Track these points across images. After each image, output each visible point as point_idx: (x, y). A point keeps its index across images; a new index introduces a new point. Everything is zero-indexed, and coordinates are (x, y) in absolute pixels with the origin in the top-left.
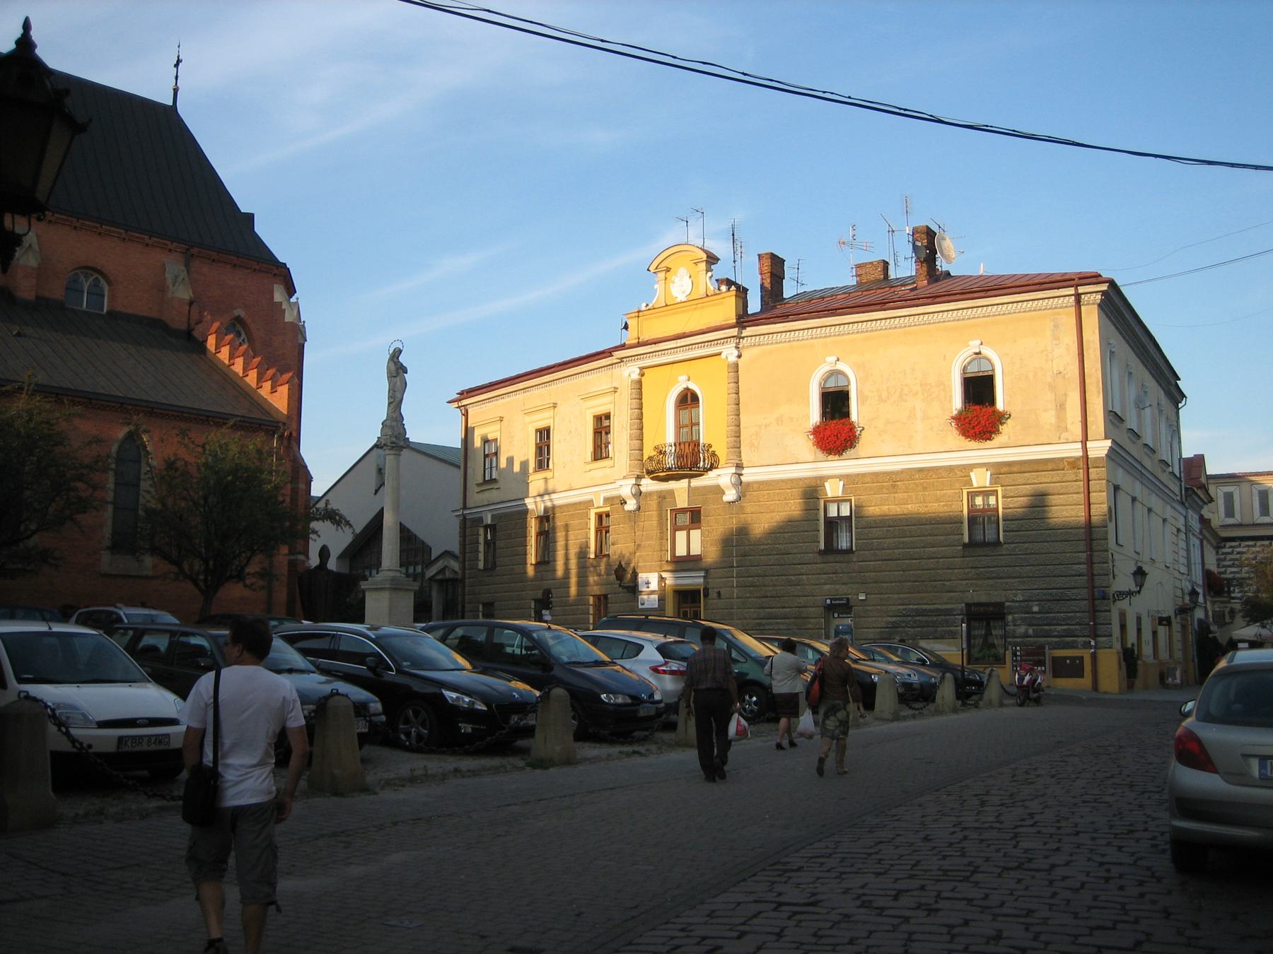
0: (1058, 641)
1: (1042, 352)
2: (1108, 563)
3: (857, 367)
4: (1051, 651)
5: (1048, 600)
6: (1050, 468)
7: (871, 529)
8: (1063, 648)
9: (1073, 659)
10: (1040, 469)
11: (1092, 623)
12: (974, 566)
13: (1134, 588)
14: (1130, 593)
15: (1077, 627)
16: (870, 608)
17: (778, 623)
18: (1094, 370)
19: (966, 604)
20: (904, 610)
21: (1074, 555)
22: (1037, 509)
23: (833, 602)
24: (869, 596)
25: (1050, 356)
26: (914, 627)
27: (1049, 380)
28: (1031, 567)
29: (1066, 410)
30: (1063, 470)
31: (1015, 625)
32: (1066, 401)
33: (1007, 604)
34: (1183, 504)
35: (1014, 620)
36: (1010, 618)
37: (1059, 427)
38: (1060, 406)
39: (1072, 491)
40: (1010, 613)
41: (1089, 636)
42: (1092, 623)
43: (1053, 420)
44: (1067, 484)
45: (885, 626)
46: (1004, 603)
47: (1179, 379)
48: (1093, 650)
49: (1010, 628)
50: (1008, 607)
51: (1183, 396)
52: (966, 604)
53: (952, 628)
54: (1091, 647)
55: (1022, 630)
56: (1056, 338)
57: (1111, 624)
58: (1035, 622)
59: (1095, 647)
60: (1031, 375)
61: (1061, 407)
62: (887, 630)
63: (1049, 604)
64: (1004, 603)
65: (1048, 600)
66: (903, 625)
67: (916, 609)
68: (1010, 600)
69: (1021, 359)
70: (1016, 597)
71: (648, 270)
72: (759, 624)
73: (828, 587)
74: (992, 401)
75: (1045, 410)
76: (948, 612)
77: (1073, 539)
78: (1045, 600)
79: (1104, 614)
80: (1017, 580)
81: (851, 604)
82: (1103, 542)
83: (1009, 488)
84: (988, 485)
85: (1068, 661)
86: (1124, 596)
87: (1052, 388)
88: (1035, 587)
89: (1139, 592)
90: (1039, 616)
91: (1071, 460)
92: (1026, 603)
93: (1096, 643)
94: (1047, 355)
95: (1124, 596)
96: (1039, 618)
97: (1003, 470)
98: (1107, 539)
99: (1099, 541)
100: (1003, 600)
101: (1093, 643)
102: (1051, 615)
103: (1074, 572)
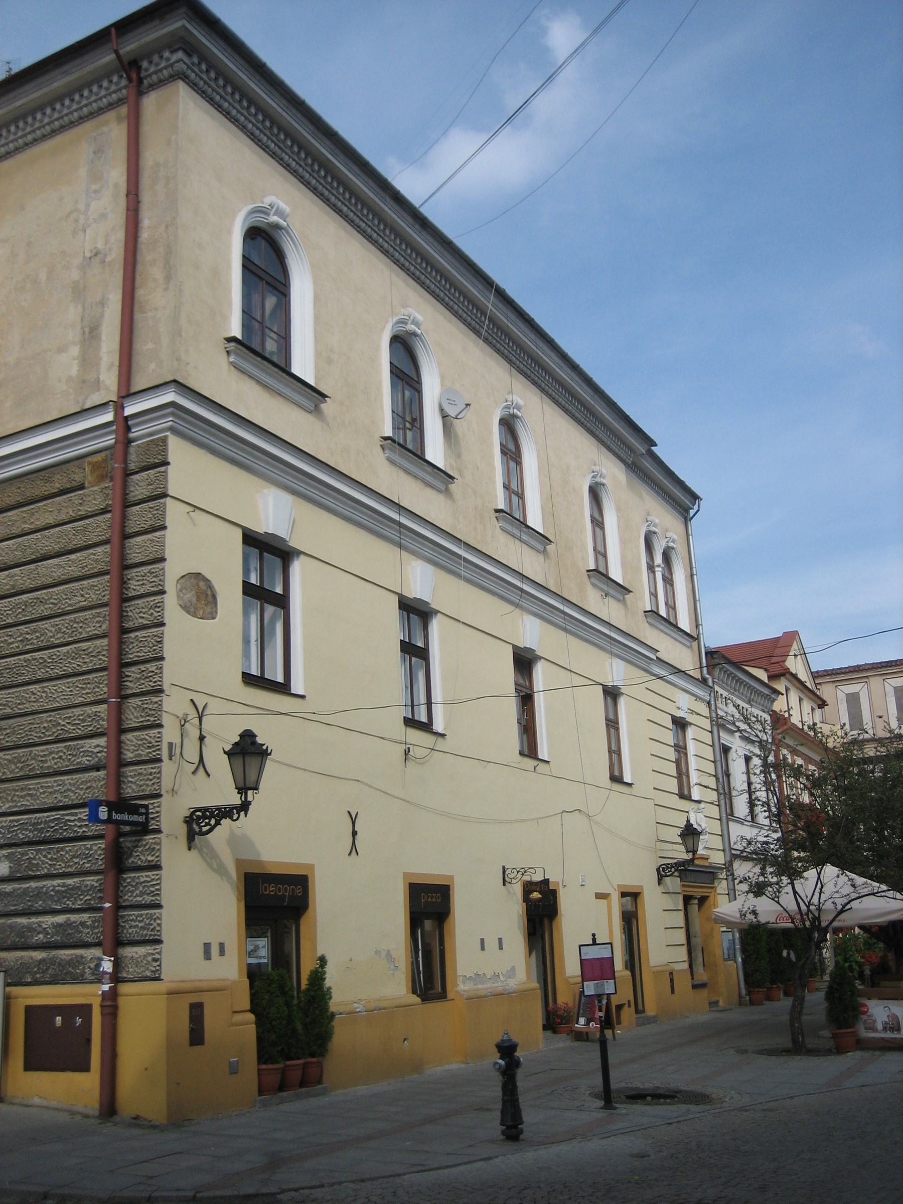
0: (42, 961)
1: (68, 216)
2: (160, 726)
5: (30, 843)
6: (57, 486)
8: (53, 982)
9: (68, 1011)
10: (37, 493)
11: (107, 905)
14: (226, 813)
15: (85, 917)
18: (162, 228)
22: (24, 597)
27: (75, 275)
29: (100, 339)
30: (82, 487)
32: (102, 316)
34: (704, 681)
37: (84, 382)
39: (96, 540)
41: (98, 944)
42: (107, 905)
43: (74, 371)
44: (87, 521)
47: (656, 445)
48: (106, 987)
51: (695, 497)
54: (99, 979)
56: (96, 176)
59: (116, 978)
60: (43, 276)
61: (91, 333)
63: (31, 852)
65: (30, 843)
69: (29, 244)
75: (62, 349)
77: (90, 666)
79: (143, 876)
82: (152, 667)
85: (59, 1020)
86: (213, 822)
87: (78, 291)
89: (244, 807)
91: (98, 458)
93: (117, 964)
94: (76, 221)
95: (213, 822)
98: (162, 658)
99: (142, 668)
101: (107, 966)
102: (33, 884)
103: (85, 761)
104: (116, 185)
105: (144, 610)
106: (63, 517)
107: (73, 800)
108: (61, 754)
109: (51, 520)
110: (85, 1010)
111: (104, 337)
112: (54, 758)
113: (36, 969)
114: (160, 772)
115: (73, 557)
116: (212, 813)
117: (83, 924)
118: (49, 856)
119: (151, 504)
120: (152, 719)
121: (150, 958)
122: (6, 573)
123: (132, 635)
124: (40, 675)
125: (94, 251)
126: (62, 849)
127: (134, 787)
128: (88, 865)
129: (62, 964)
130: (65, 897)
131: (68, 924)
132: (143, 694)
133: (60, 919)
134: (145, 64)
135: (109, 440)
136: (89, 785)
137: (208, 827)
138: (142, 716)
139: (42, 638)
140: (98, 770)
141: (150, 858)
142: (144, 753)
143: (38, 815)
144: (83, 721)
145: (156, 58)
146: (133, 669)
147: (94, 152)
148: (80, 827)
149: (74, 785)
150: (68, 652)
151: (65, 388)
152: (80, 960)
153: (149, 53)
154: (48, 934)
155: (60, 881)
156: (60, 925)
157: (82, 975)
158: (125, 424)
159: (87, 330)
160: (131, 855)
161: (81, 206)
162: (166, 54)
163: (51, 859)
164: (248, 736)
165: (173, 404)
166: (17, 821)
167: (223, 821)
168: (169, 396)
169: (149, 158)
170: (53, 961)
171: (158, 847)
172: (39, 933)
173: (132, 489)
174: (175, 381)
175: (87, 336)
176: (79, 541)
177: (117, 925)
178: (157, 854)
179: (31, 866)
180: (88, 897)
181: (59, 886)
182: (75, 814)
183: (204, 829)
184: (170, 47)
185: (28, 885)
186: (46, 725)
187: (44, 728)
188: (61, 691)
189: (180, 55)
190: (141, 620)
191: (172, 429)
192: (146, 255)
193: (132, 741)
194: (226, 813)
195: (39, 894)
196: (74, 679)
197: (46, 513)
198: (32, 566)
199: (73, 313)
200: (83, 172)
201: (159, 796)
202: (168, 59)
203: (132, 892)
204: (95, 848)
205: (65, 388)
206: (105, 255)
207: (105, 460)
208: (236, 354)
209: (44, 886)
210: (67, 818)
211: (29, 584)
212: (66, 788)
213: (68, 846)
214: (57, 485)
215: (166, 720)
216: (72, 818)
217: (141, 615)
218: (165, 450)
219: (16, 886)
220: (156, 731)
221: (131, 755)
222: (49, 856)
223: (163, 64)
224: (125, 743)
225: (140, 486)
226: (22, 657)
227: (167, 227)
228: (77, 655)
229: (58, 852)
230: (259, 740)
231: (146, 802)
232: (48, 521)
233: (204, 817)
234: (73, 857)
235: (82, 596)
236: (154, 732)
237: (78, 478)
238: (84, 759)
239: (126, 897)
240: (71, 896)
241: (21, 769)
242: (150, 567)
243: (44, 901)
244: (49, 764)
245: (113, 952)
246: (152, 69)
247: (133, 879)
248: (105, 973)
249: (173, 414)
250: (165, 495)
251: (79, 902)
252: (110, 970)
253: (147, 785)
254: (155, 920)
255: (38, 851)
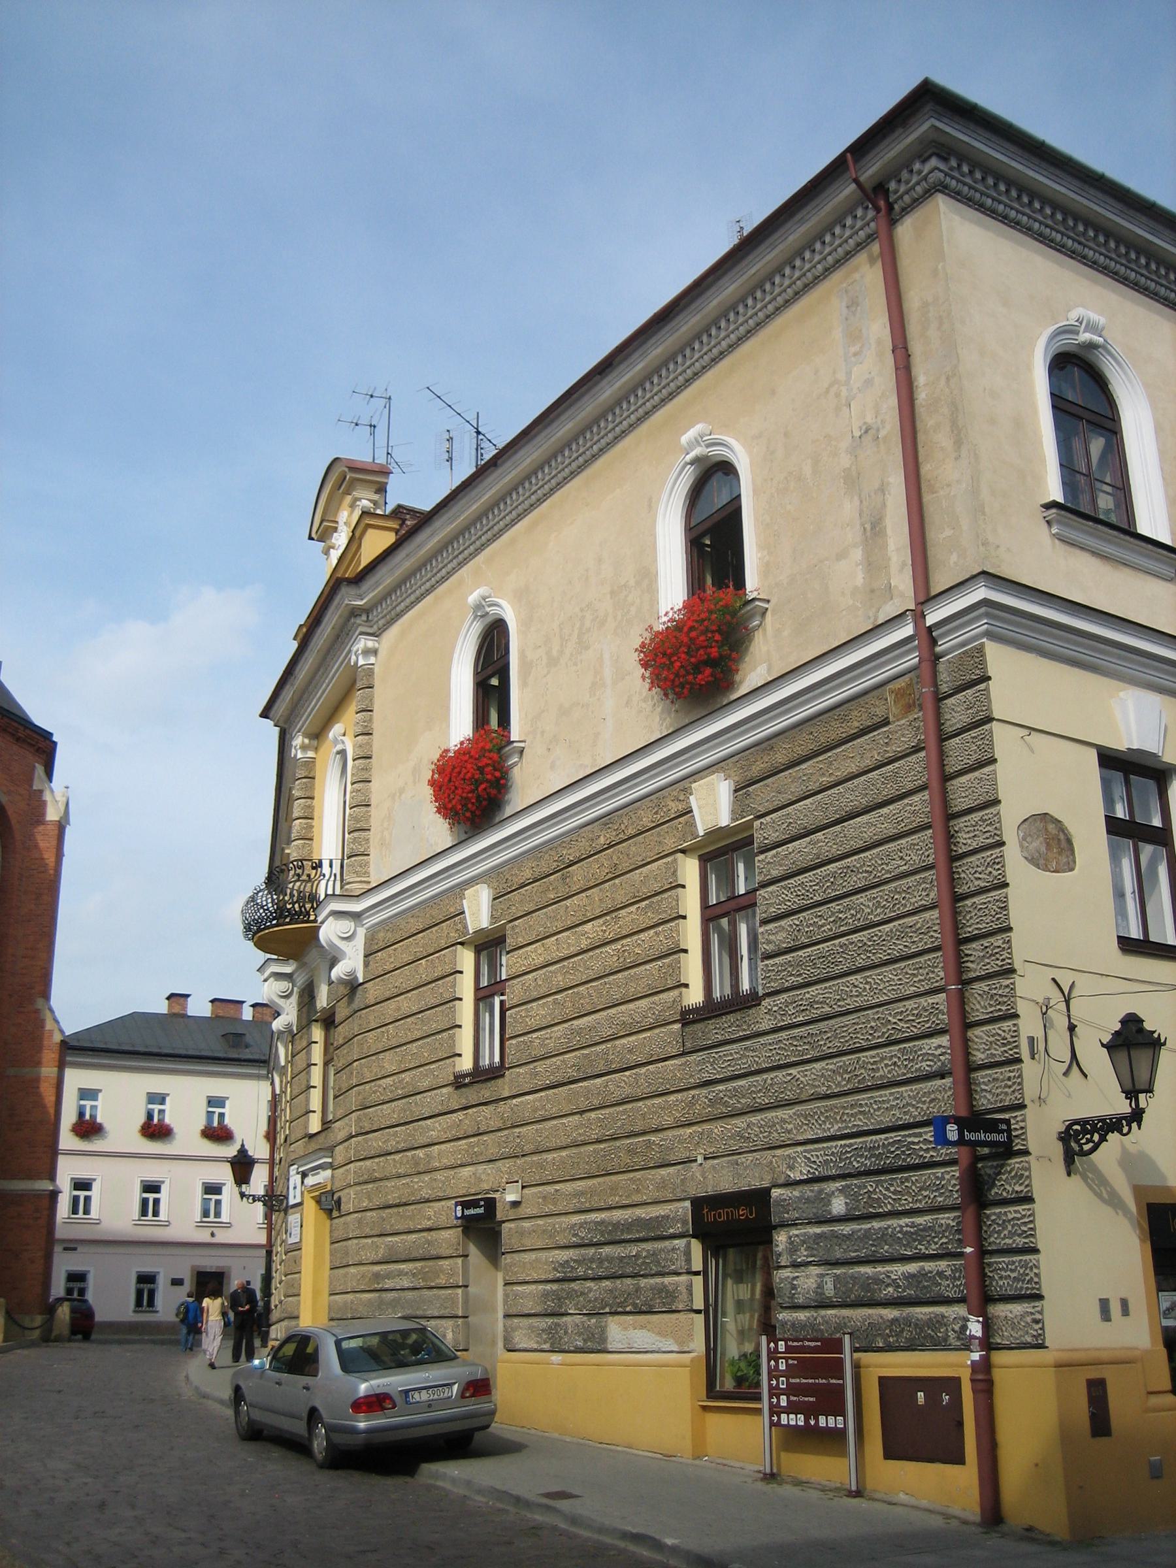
0: (895, 1321)
1: (827, 391)
2: (1016, 1016)
3: (521, 596)
4: (866, 1358)
5: (868, 1173)
6: (855, 725)
7: (529, 1006)
8: (911, 1347)
12: (706, 1077)
13: (1123, 1107)
14: (1112, 1125)
15: (942, 1264)
16: (526, 1224)
17: (401, 1273)
18: (943, 382)
19: (698, 1203)
20: (581, 1225)
21: (923, 1001)
22: (832, 867)
23: (467, 1212)
24: (526, 1191)
25: (844, 393)
26: (601, 1278)
27: (845, 461)
28: (823, 1064)
31: (795, 1265)
32: (884, 505)
33: (775, 1193)
35: (793, 1248)
36: (781, 1239)
37: (872, 591)
38: (873, 527)
39: (910, 786)
40: (783, 1225)
41: (962, 1300)
42: (969, 1250)
43: (859, 579)
44: (897, 765)
45: (551, 1277)
46: (767, 1191)
48: (976, 1356)
49: (782, 1275)
50: (779, 1202)
52: (698, 1203)
53: (667, 1280)
55: (808, 1281)
56: (854, 336)
57: (1035, 1251)
58: (838, 1254)
59: (988, 1344)
60: (807, 470)
62: (555, 1287)
63: (870, 1183)
64: (767, 1191)
65: (868, 1173)
66: (580, 1271)
67: (602, 1222)
68: (781, 1180)
69: (786, 435)
70: (791, 1168)
71: (311, 538)
72: (377, 1276)
73: (466, 1171)
74: (740, 583)
75: (842, 555)
76: (654, 1232)
77: (921, 946)
78: (859, 1174)
79: (1012, 1211)
80: (790, 1112)
81: (500, 1216)
82: (997, 940)
83: (768, 818)
84: (724, 820)
86: (1096, 1137)
87: (852, 480)
88: (834, 1130)
89: (1137, 1116)
90: (846, 1229)
91: (901, 683)
92: (816, 1187)
93: (987, 1326)
94: (838, 395)
96: (848, 1237)
97: (756, 769)
98: (1009, 929)
99: (985, 943)
100: (766, 1184)
101: (975, 1328)
102: (876, 1224)
103: (926, 1066)
104: (879, 342)
105: (979, 869)
106: (868, 762)
107: (915, 1117)
108: (895, 1060)
109: (853, 769)
110: (953, 1384)
111: (889, 532)
112: (887, 1065)
113: (887, 1331)
114: (1020, 1076)
115: (885, 811)
116: (1094, 1126)
117: (940, 1274)
118: (892, 1189)
119: (973, 733)
120: (1004, 1008)
121: (1029, 1319)
122: (808, 839)
123: (969, 902)
124: (860, 962)
125: (864, 428)
126: (907, 1179)
127: (989, 1096)
128: (940, 1199)
129: (919, 1326)
130: (915, 1240)
131: (922, 1275)
132: (989, 976)
133: (912, 1268)
134: (892, 185)
135: (912, 660)
136: (933, 1096)
137: (1091, 1145)
138: (991, 1006)
139: (859, 916)
140: (943, 1077)
141: (1017, 1188)
142: (998, 1053)
143: (874, 1138)
144: (919, 1015)
145: (905, 175)
146: (974, 946)
147: (848, 307)
148: (927, 1150)
149: (914, 1098)
150: (891, 931)
151: (851, 602)
152: (940, 1321)
153: (894, 173)
154: (899, 1286)
155: (907, 1220)
156: (912, 1276)
157: (946, 1339)
158: (930, 636)
159: (868, 526)
160: (994, 1185)
161: (841, 376)
162: (917, 166)
163: (895, 1192)
164: (1132, 1022)
165: (985, 602)
166: (850, 1145)
167: (1110, 1136)
168: (980, 593)
169: (913, 300)
170: (908, 1321)
171: (1027, 1174)
172: (888, 1285)
173: (948, 716)
174: (984, 573)
175: (868, 534)
176: (889, 791)
177: (983, 1276)
178: (1026, 1183)
179: (871, 1202)
180: (944, 1240)
181: (907, 1226)
182: (920, 1135)
183: (1086, 1147)
184: (920, 157)
185: (869, 1226)
186: (873, 1024)
187: (872, 1027)
188: (888, 981)
189: (934, 162)
190: (977, 883)
191: (988, 634)
192: (927, 421)
193: (981, 1038)
194: (1112, 1125)
195: (884, 1237)
196: (903, 964)
197: (847, 760)
198: (838, 828)
199: (849, 508)
200: (838, 334)
201: (1022, 1106)
202: (920, 172)
203: (999, 1232)
204: (947, 1177)
205: (851, 602)
206: (878, 430)
207: (910, 685)
208: (1059, 522)
209: (889, 1226)
210: (909, 1140)
211: (835, 851)
212: (904, 1102)
213: (914, 1175)
214: (856, 724)
215: (1022, 1008)
216: (916, 1140)
217: (977, 875)
218: (983, 662)
219: (855, 1226)
220: (1010, 1023)
221: (983, 1056)
222: (892, 1189)
223: (915, 179)
224: (973, 1041)
225: (957, 712)
226: (836, 942)
227: (948, 379)
228: (902, 934)
229: (902, 1183)
230: (1148, 1026)
231: (1007, 1116)
232: (850, 770)
233: (1085, 1132)
234: (921, 1189)
235: (901, 858)
236: (1007, 1025)
237: (880, 712)
238: (924, 1064)
239: (992, 1239)
240: (924, 1238)
241: (849, 1081)
242: (981, 814)
243: (890, 1245)
244: (881, 1073)
245: (982, 1312)
246: (902, 189)
247: (999, 1215)
248: (973, 1337)
249: (987, 615)
250: (989, 719)
251: (933, 1247)
252: (979, 1334)
253: (1006, 1094)
254: (1031, 1269)
255: (878, 1183)
